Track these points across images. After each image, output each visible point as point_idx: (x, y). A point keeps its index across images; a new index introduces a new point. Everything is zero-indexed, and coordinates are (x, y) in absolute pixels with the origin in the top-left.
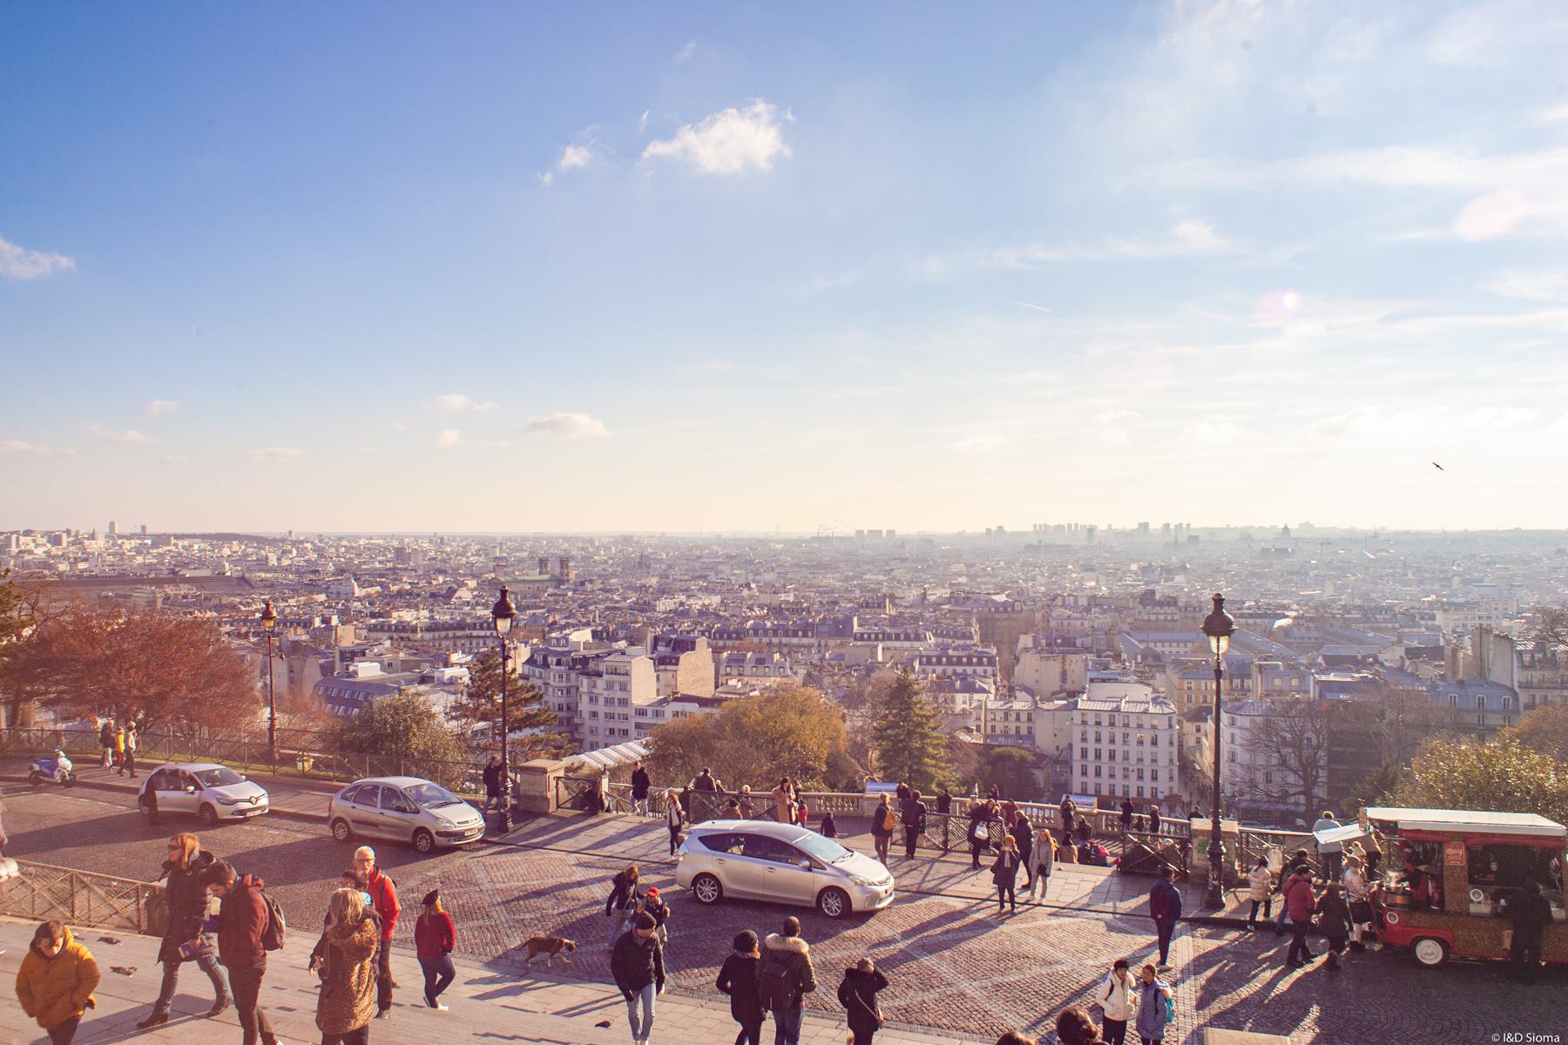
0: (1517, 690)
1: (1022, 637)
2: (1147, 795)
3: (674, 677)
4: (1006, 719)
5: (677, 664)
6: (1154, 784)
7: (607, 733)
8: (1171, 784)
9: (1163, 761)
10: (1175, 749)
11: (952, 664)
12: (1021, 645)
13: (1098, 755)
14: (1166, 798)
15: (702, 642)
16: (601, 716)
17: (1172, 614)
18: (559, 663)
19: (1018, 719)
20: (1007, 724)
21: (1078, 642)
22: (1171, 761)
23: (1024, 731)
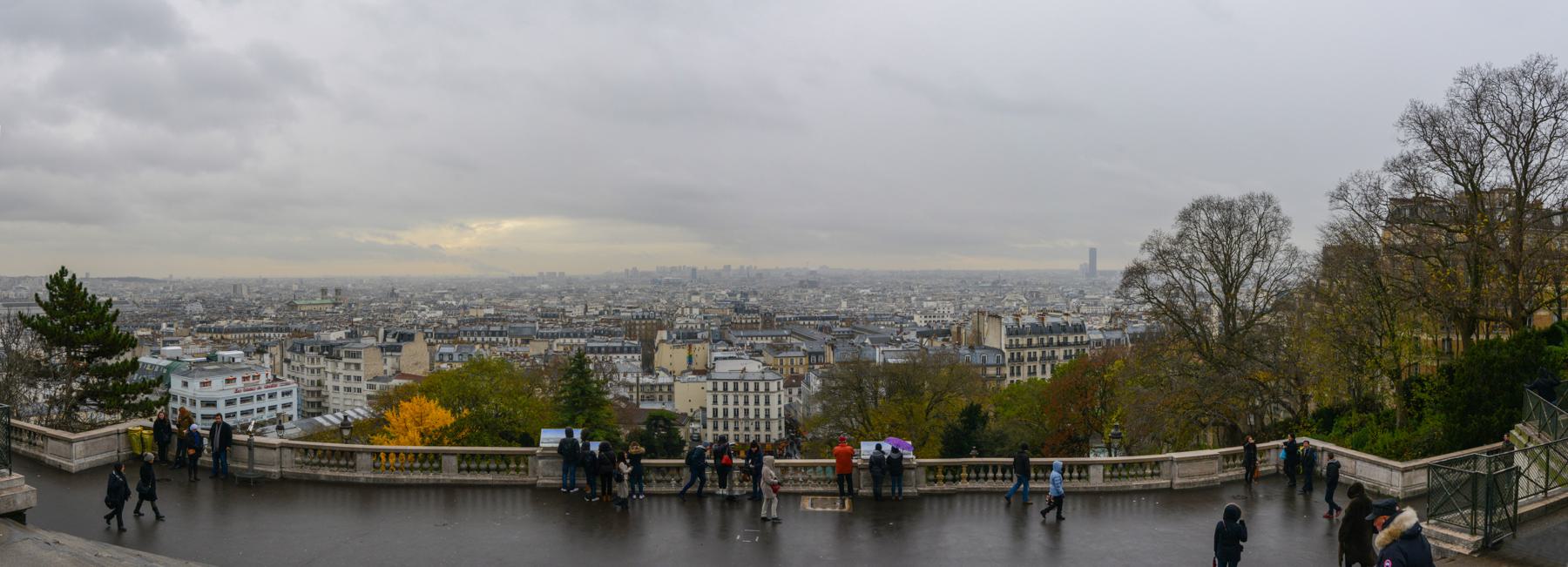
0: (1004, 349)
1: (659, 332)
5: (400, 351)
6: (768, 433)
9: (774, 415)
10: (782, 406)
11: (611, 353)
13: (726, 413)
14: (777, 441)
15: (419, 337)
16: (341, 390)
18: (312, 350)
19: (660, 390)
21: (699, 336)
22: (780, 415)
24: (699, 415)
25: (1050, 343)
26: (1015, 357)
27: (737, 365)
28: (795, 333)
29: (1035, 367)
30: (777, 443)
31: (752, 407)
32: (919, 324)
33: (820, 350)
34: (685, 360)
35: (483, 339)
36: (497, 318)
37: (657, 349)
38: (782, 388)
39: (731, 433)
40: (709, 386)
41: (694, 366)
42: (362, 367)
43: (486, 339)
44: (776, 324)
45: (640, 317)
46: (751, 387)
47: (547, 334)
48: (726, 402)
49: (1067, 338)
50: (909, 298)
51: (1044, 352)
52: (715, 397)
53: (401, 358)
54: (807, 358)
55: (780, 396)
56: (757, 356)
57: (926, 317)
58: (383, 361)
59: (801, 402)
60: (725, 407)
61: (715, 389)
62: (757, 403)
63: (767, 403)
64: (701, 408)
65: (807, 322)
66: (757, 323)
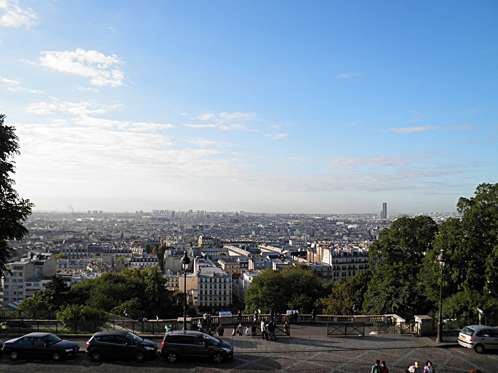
2: (223, 305)
3: (41, 269)
7: (13, 294)
9: (228, 293)
10: (231, 289)
13: (206, 293)
22: (230, 293)
23: (175, 285)
25: (353, 262)
26: (336, 267)
29: (345, 272)
31: (218, 289)
35: (74, 254)
38: (231, 281)
42: (23, 274)
43: (75, 253)
44: (220, 245)
48: (206, 287)
51: (350, 266)
52: (201, 285)
53: (43, 268)
54: (240, 265)
55: (230, 284)
58: (34, 271)
59: (239, 287)
60: (206, 289)
61: (201, 281)
62: (220, 288)
63: (225, 288)
65: (236, 244)
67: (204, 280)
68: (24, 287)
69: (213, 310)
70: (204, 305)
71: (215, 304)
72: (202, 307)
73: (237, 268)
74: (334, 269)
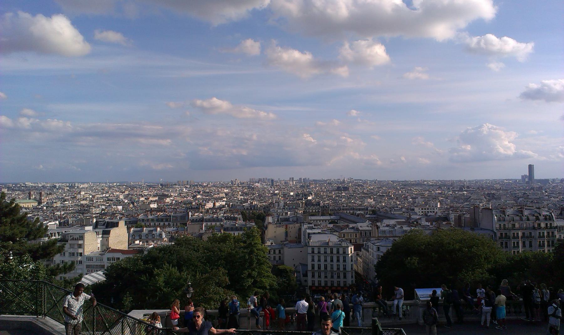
0: (495, 230)
2: (342, 285)
3: (107, 240)
4: (270, 253)
6: (345, 280)
8: (352, 279)
9: (349, 268)
11: (238, 230)
12: (266, 222)
13: (319, 267)
15: (122, 223)
17: (318, 209)
19: (274, 253)
20: (269, 256)
21: (291, 220)
23: (277, 258)
24: (300, 268)
27: (325, 238)
28: (343, 218)
29: (518, 243)
30: (351, 287)
31: (335, 263)
32: (418, 214)
33: (367, 228)
34: (284, 235)
36: (158, 210)
37: (266, 228)
38: (353, 252)
39: (323, 280)
40: (310, 250)
41: (289, 239)
45: (249, 208)
46: (335, 251)
47: (197, 219)
48: (319, 260)
49: (539, 225)
50: (406, 197)
51: (524, 233)
52: (313, 257)
56: (334, 232)
57: (422, 209)
60: (319, 263)
61: (313, 252)
62: (338, 261)
63: (344, 261)
64: (300, 263)
65: (348, 212)
66: (318, 211)
67: (316, 251)
68: (84, 262)
69: (329, 292)
70: (316, 284)
71: (332, 282)
72: (314, 288)
73: (356, 237)
74: (501, 237)
